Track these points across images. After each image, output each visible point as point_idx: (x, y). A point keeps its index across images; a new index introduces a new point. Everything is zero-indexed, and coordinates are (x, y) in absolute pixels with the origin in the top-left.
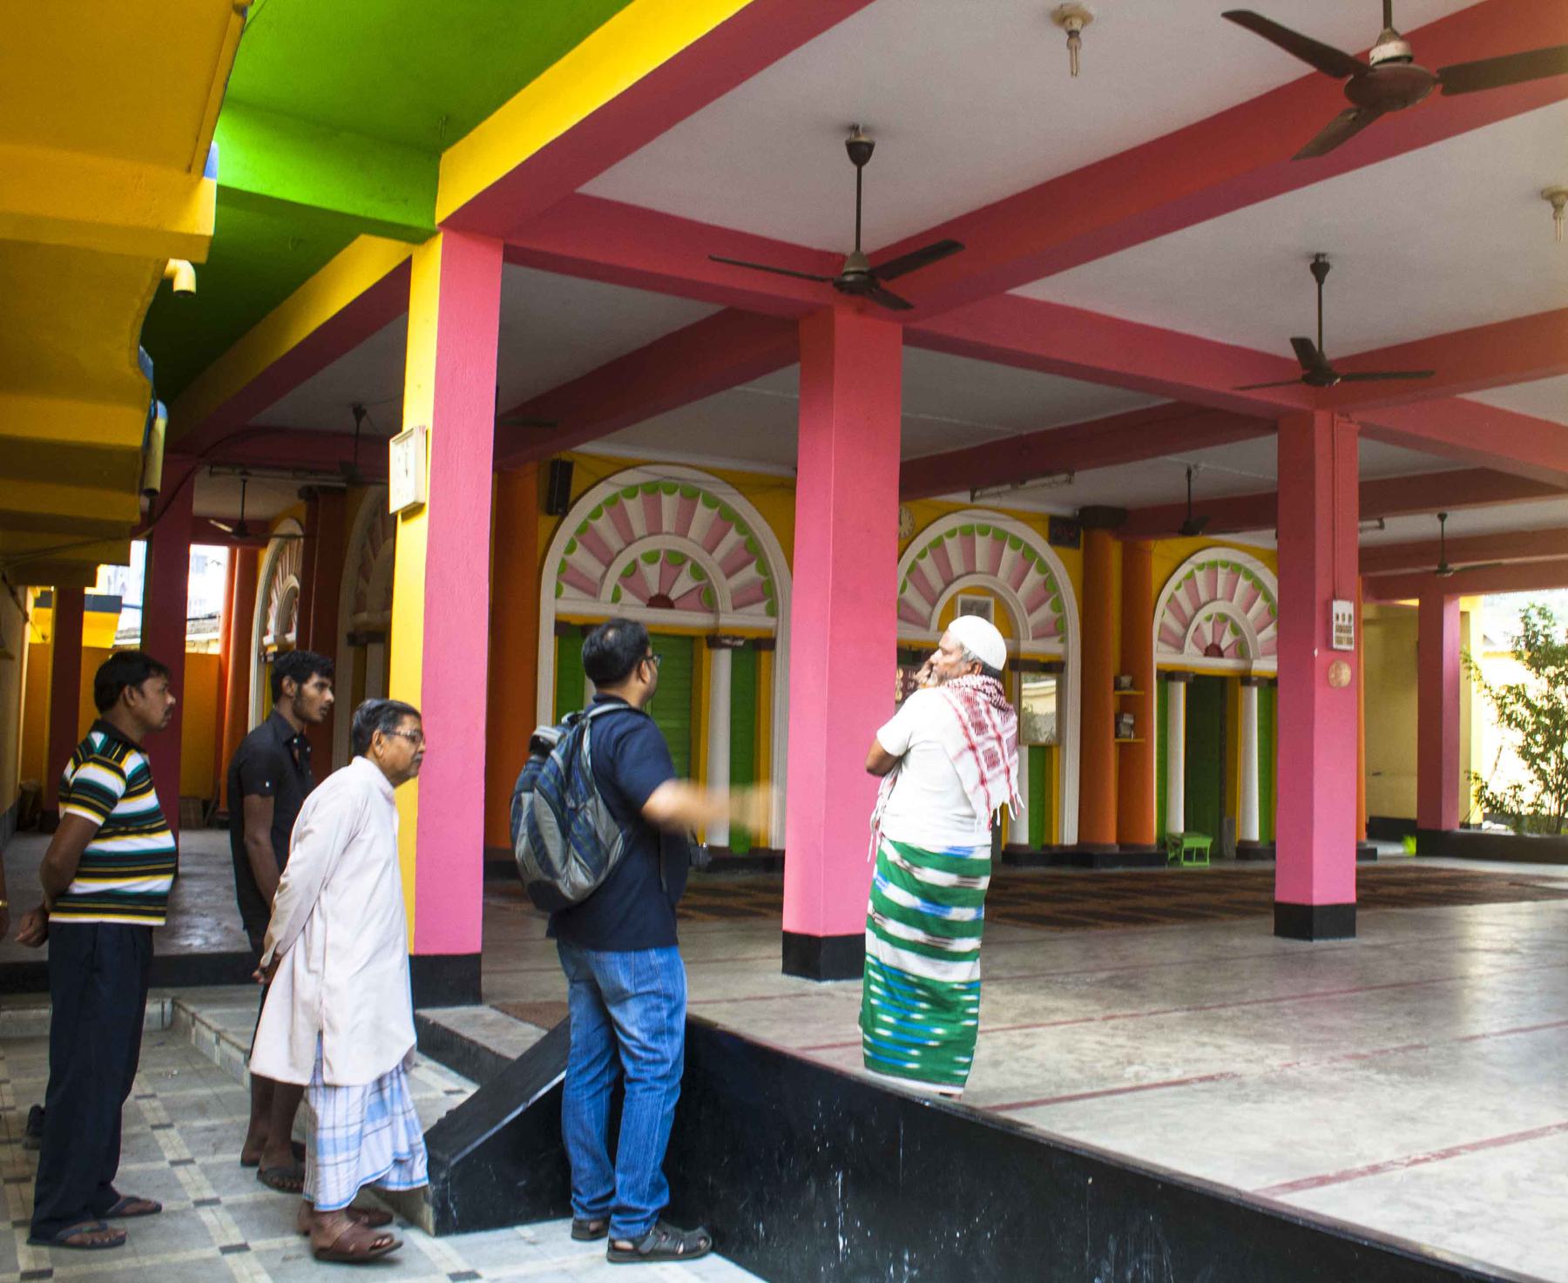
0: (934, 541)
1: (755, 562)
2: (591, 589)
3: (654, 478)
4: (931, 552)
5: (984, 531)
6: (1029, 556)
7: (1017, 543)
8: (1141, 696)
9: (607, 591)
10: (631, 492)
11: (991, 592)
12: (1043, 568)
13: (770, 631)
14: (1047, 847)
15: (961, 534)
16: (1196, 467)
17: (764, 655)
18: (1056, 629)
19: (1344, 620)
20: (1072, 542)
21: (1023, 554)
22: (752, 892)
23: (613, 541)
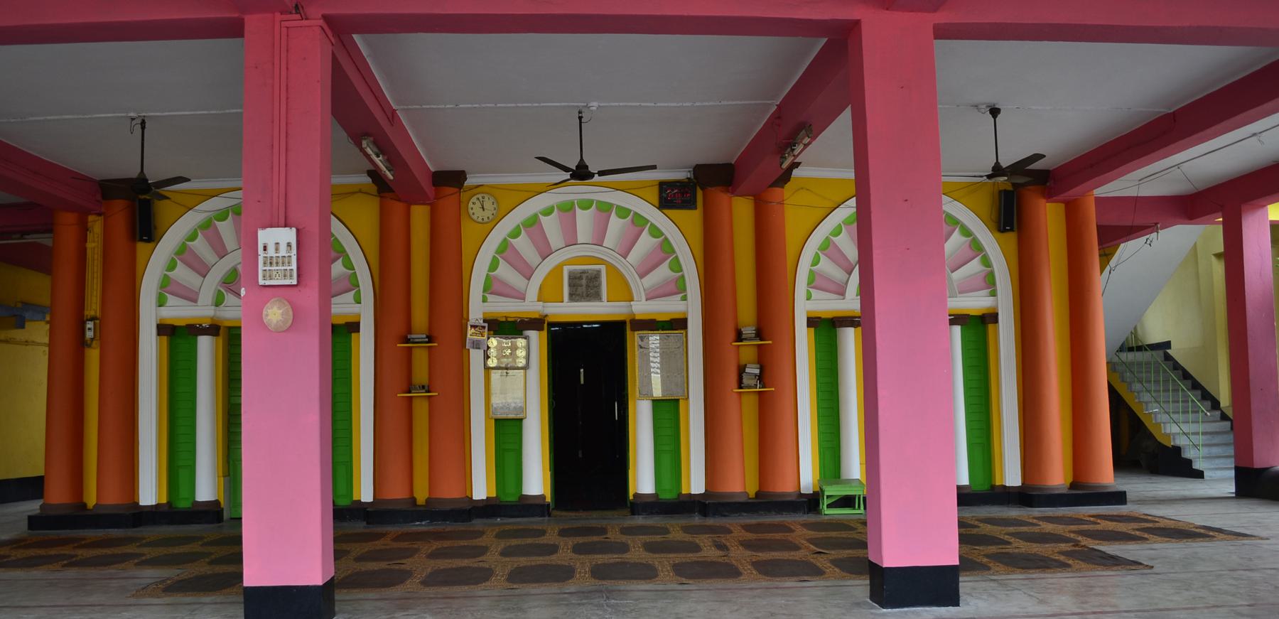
0: (529, 219)
1: (341, 259)
2: (192, 297)
3: (236, 202)
4: (526, 231)
5: (586, 205)
6: (639, 223)
7: (623, 212)
8: (769, 344)
9: (206, 296)
10: (222, 215)
11: (602, 262)
12: (656, 232)
13: (994, 309)
14: (993, 487)
15: (559, 209)
16: (587, 107)
17: (354, 335)
18: (989, 283)
19: (277, 250)
20: (689, 204)
21: (632, 221)
22: (1099, 521)
23: (206, 253)
